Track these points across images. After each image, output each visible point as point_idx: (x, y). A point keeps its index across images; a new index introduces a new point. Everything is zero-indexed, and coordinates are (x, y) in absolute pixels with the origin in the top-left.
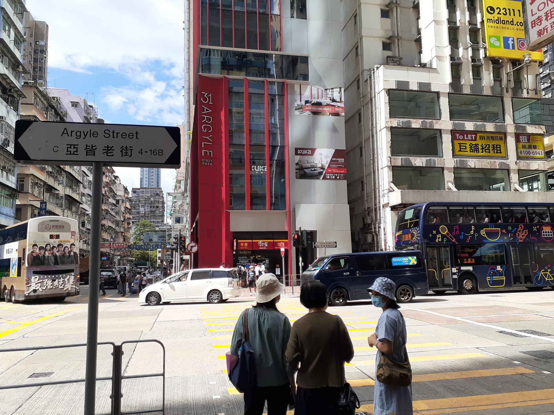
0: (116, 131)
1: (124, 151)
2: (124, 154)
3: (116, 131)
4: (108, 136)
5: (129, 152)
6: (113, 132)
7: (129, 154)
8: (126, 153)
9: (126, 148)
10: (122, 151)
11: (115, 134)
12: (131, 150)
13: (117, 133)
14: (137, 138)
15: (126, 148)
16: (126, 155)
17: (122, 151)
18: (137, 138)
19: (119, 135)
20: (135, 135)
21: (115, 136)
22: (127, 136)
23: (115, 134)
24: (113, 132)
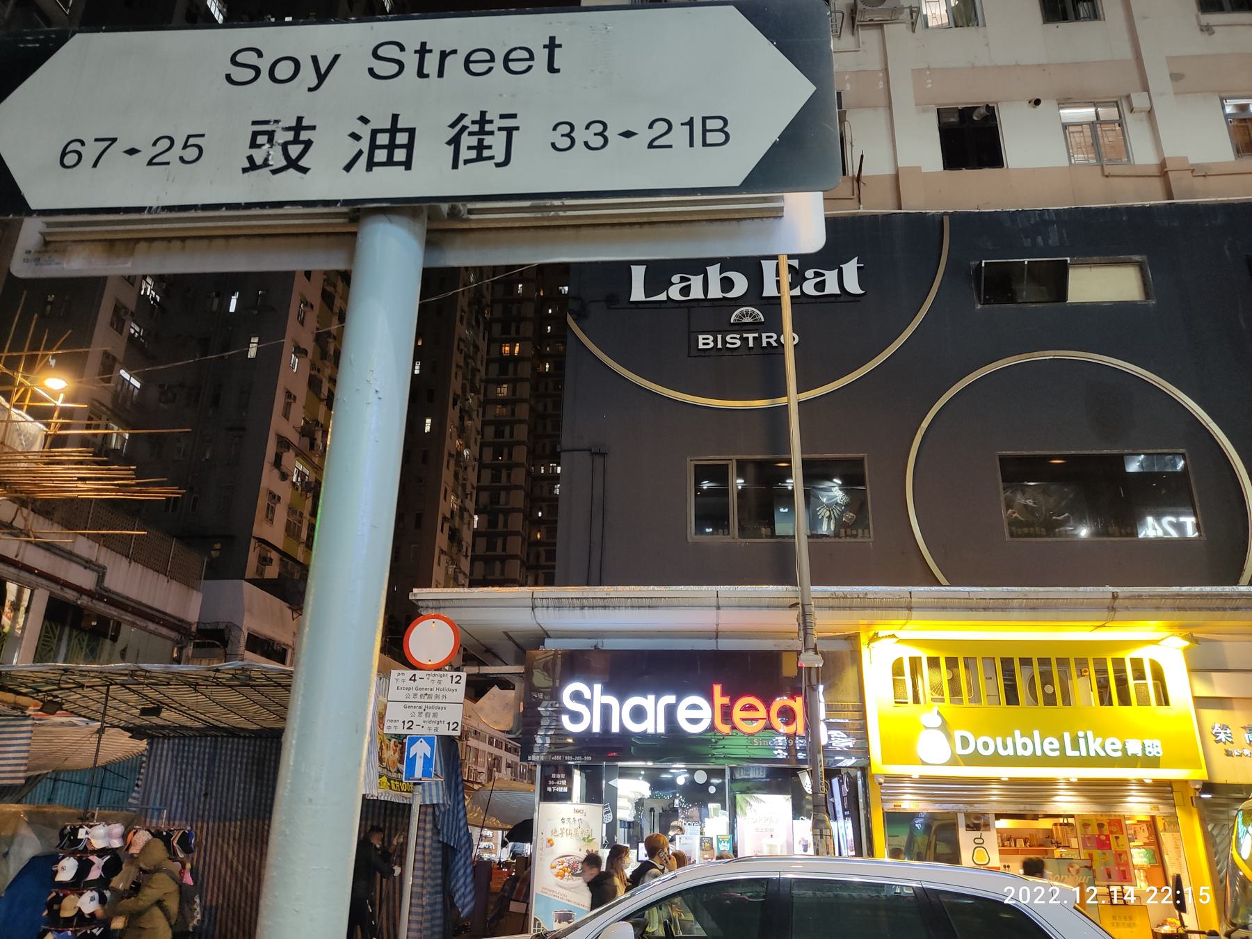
0: (436, 46)
1: (467, 141)
2: (465, 154)
3: (436, 46)
5: (497, 143)
8: (480, 147)
9: (483, 120)
10: (455, 141)
12: (510, 131)
13: (444, 55)
14: (552, 69)
15: (483, 120)
17: (455, 141)
18: (552, 69)
20: (542, 55)
22: (498, 64)
24: (423, 51)
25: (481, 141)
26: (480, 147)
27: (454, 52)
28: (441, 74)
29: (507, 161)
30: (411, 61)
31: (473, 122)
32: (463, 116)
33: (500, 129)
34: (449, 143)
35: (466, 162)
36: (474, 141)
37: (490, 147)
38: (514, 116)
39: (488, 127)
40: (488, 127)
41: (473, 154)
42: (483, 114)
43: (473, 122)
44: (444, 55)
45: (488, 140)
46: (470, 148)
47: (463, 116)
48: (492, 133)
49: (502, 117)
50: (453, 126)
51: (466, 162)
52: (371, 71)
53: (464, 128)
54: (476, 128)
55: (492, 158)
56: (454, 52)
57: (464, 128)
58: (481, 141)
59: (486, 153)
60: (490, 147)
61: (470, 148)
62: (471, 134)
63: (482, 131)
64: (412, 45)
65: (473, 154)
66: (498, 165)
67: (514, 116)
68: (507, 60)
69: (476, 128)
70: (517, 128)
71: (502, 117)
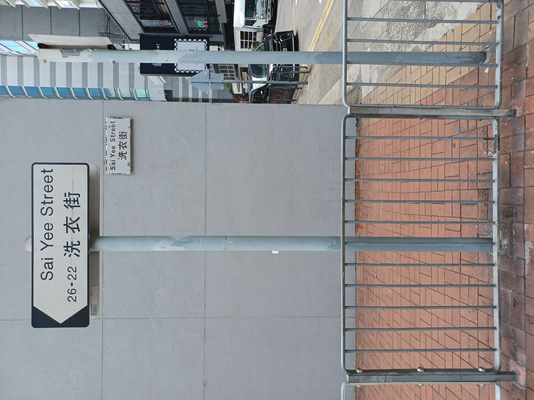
1: (72, 204)
2: (76, 204)
7: (75, 197)
8: (74, 201)
9: (67, 201)
10: (72, 207)
12: (69, 194)
15: (67, 201)
16: (77, 201)
26: (74, 201)
35: (78, 204)
36: (72, 203)
39: (68, 199)
40: (68, 199)
41: (76, 203)
45: (72, 199)
47: (65, 206)
49: (65, 196)
50: (68, 208)
51: (78, 204)
53: (68, 205)
54: (68, 203)
57: (68, 205)
59: (76, 199)
63: (70, 201)
65: (76, 203)
69: (68, 203)
71: (65, 196)
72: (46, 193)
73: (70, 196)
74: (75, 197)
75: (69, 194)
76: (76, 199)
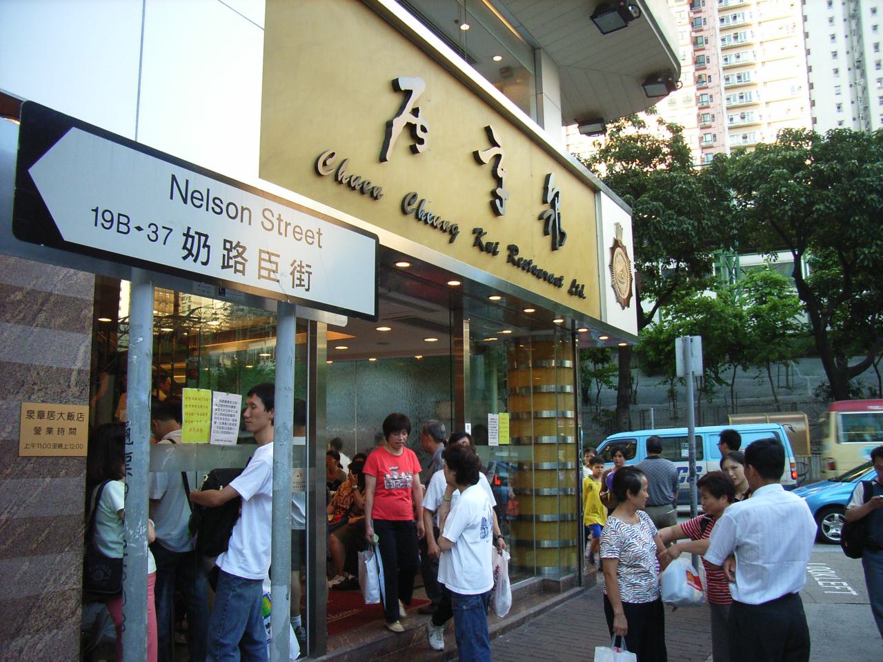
1: (297, 275)
4: (269, 225)
5: (305, 277)
6: (280, 220)
8: (301, 279)
10: (293, 273)
11: (283, 225)
12: (310, 273)
15: (301, 266)
16: (300, 285)
18: (320, 247)
19: (290, 229)
20: (316, 236)
21: (283, 231)
22: (304, 236)
23: (283, 225)
24: (280, 220)
25: (301, 276)
27: (290, 224)
28: (286, 236)
29: (308, 290)
30: (276, 223)
31: (298, 266)
32: (295, 261)
33: (306, 272)
34: (291, 274)
35: (297, 285)
37: (303, 280)
38: (310, 267)
40: (303, 270)
42: (301, 262)
43: (298, 266)
44: (287, 224)
46: (298, 279)
47: (295, 261)
48: (303, 273)
50: (292, 265)
51: (297, 285)
52: (262, 223)
53: (295, 267)
54: (298, 269)
55: (304, 286)
56: (290, 224)
57: (295, 267)
58: (301, 276)
60: (303, 280)
61: (298, 279)
62: (298, 271)
64: (276, 216)
65: (297, 282)
66: (308, 290)
67: (310, 267)
68: (306, 236)
69: (298, 269)
70: (311, 273)
72: (293, 226)
73: (307, 274)
74: (305, 283)
75: (310, 273)
76: (303, 283)
